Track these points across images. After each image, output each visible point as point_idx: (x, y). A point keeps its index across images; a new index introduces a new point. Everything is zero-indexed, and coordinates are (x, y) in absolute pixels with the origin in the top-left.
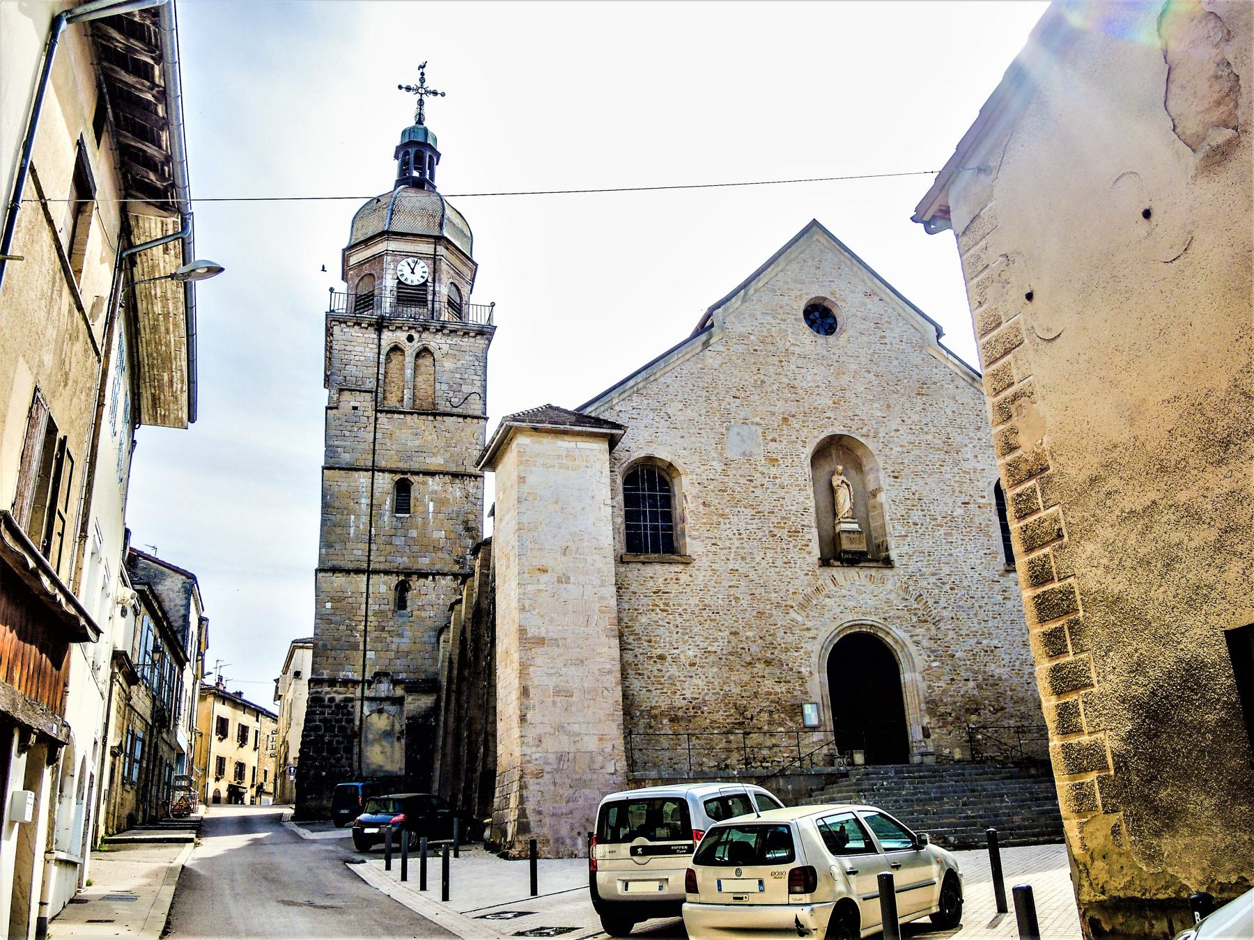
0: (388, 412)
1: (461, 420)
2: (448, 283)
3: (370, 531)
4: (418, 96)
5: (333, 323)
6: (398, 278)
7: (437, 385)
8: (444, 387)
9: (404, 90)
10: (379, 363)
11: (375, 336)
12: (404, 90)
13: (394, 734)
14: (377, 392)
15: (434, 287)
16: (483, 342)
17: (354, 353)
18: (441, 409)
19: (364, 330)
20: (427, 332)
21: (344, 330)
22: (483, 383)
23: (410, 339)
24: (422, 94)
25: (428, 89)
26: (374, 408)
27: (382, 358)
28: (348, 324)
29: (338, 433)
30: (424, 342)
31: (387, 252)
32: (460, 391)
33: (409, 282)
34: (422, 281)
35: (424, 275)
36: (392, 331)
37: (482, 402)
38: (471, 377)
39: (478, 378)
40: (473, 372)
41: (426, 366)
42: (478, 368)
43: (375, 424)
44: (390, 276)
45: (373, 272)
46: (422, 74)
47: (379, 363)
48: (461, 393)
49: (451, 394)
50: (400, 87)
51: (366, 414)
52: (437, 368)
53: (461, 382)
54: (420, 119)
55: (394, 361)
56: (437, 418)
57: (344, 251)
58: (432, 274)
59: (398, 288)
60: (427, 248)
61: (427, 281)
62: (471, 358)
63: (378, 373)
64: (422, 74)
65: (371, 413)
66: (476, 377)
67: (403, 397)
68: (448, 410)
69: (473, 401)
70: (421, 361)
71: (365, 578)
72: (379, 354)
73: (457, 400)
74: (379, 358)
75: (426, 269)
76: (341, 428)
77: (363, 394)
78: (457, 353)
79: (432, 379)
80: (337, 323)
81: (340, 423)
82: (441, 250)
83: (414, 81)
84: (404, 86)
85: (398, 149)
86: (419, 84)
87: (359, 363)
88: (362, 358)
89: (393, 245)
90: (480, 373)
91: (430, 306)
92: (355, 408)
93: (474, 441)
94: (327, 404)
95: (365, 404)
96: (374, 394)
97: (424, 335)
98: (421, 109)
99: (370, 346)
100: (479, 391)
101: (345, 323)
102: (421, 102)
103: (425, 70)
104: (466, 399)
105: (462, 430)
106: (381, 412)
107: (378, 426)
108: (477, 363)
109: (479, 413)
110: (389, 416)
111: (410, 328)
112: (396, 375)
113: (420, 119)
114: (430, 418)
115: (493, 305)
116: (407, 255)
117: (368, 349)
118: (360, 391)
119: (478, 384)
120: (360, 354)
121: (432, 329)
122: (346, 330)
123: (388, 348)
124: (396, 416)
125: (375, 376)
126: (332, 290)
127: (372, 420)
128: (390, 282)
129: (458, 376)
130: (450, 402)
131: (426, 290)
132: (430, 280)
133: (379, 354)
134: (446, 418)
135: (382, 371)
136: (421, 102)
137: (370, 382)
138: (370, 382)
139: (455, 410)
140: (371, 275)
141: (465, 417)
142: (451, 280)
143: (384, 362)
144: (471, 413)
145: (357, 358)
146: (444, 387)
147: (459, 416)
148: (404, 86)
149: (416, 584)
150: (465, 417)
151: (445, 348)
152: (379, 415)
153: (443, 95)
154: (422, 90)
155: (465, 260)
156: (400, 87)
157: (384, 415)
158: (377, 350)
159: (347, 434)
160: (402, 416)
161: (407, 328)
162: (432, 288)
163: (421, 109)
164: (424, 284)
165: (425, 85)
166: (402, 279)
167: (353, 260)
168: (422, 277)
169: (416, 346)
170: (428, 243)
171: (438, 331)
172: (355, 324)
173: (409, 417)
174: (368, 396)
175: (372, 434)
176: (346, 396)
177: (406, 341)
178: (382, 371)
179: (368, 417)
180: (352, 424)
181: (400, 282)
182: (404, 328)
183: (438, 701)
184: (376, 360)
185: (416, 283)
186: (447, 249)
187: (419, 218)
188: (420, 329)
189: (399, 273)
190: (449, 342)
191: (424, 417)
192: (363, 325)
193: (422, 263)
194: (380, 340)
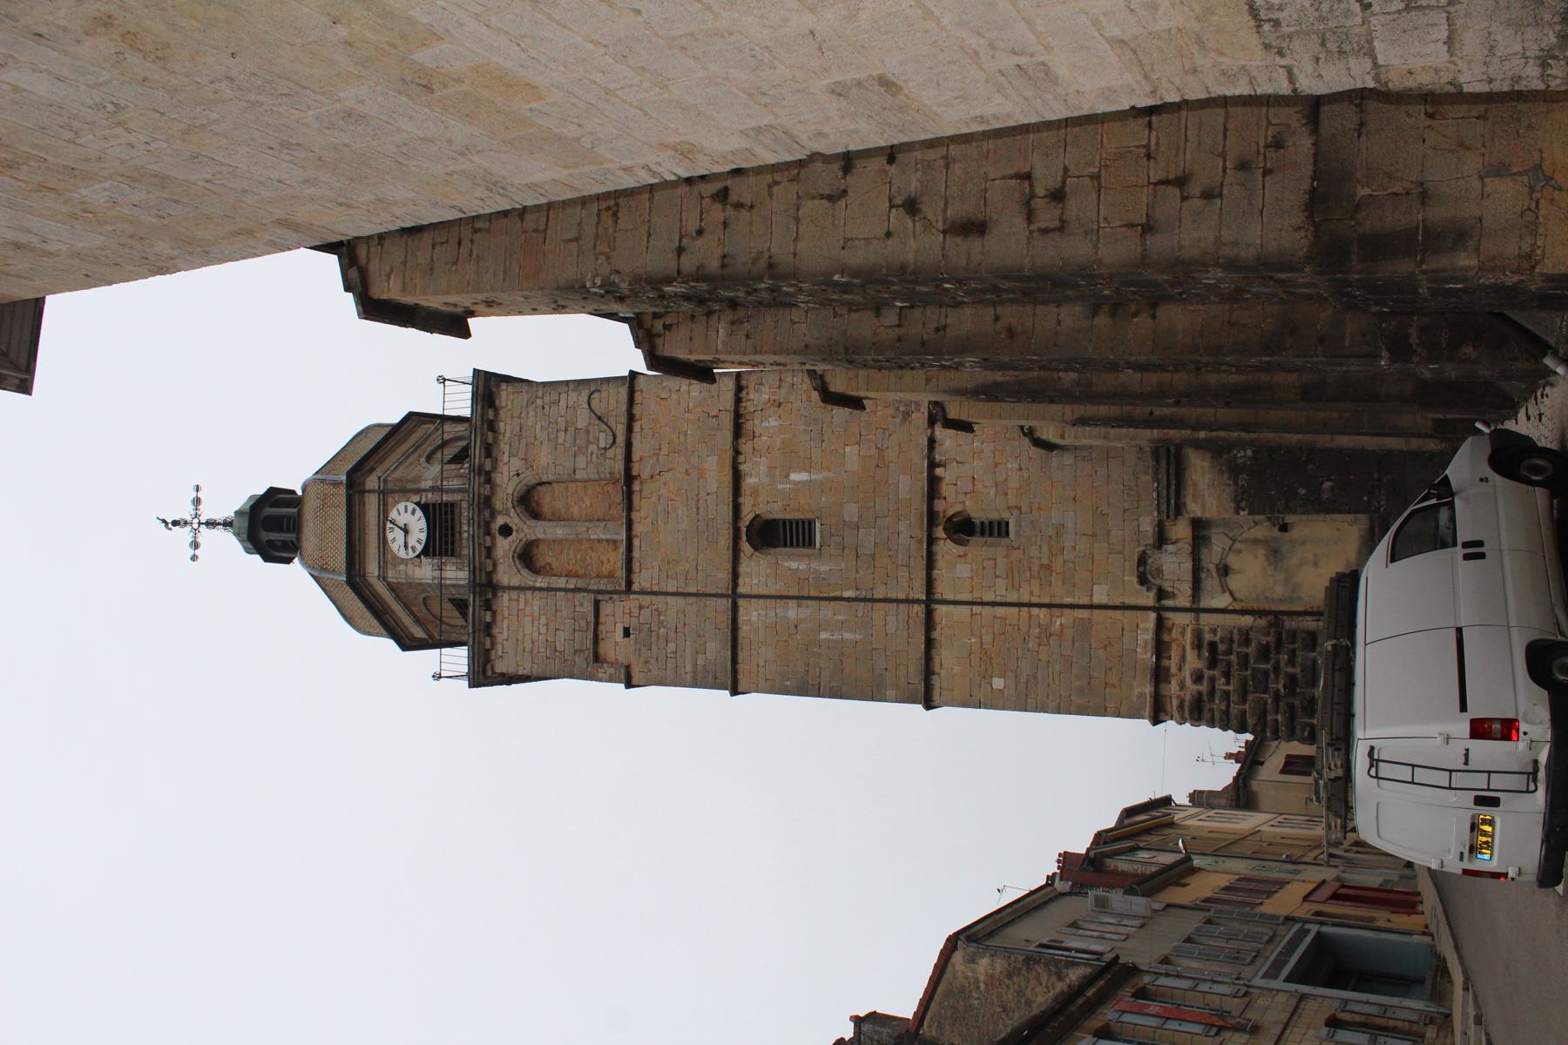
0: (629, 570)
1: (637, 427)
2: (425, 465)
3: (849, 600)
4: (203, 528)
5: (489, 673)
6: (418, 556)
7: (579, 476)
8: (581, 462)
9: (197, 552)
10: (548, 589)
11: (506, 596)
12: (197, 552)
13: (1275, 539)
14: (598, 592)
15: (426, 491)
16: (504, 394)
17: (536, 634)
18: (619, 466)
19: (499, 617)
20: (494, 500)
21: (500, 652)
22: (571, 387)
23: (506, 531)
24: (200, 523)
25: (193, 513)
26: (624, 597)
27: (540, 582)
28: (488, 645)
29: (671, 664)
30: (510, 505)
31: (383, 577)
32: (588, 432)
33: (423, 536)
34: (419, 513)
35: (410, 510)
36: (495, 565)
37: (605, 386)
38: (563, 411)
39: (564, 396)
40: (554, 408)
41: (553, 498)
42: (547, 399)
43: (652, 593)
44: (417, 569)
45: (420, 600)
46: (175, 523)
47: (548, 589)
48: (591, 429)
49: (593, 448)
50: (194, 558)
51: (635, 612)
52: (551, 478)
53: (571, 429)
54: (227, 524)
55: (548, 560)
56: (635, 473)
57: (405, 646)
58: (407, 495)
59: (434, 555)
60: (372, 503)
61: (418, 504)
62: (532, 414)
63: (565, 590)
64: (175, 523)
65: (633, 602)
66: (563, 403)
67: (608, 541)
68: (619, 451)
69: (604, 405)
70: (546, 509)
71: (941, 610)
72: (534, 589)
73: (602, 436)
74: (540, 589)
75: (401, 506)
76: (662, 659)
77: (602, 619)
78: (523, 442)
79: (572, 486)
80: (489, 666)
81: (653, 660)
82: (372, 482)
83: (184, 534)
84: (192, 552)
85: (268, 558)
86: (188, 528)
87: (552, 625)
88: (543, 620)
89: (372, 569)
90: (555, 396)
91: (456, 497)
92: (627, 632)
93: (674, 397)
94: (623, 685)
95: (619, 614)
96: (600, 597)
97: (498, 505)
98: (219, 524)
99: (521, 607)
100: (585, 393)
101: (488, 651)
102: (211, 524)
103: (169, 521)
104: (600, 418)
105: (655, 421)
106: (629, 583)
107: (655, 589)
108: (539, 402)
109: (624, 391)
110: (636, 567)
111: (488, 532)
112: (571, 554)
113: (227, 524)
114: (636, 486)
115: (443, 380)
116: (383, 541)
117: (528, 610)
118: (597, 623)
119: (573, 396)
120: (536, 623)
121: (486, 490)
122: (499, 648)
123: (524, 572)
124: (636, 554)
125: (570, 595)
126: (438, 677)
127: (646, 600)
128: (426, 572)
129: (562, 435)
130: (605, 449)
131: (434, 505)
132: (417, 499)
133: (534, 589)
134: (635, 457)
135: (561, 582)
136: (211, 524)
137: (582, 605)
138: (582, 605)
139: (621, 439)
140: (424, 599)
141: (631, 418)
142: (423, 460)
143: (547, 579)
144: (623, 407)
145: (543, 630)
146: (581, 462)
147: (630, 429)
148: (192, 552)
149: (952, 502)
150: (631, 418)
151: (516, 464)
152: (636, 587)
153: (198, 489)
154: (192, 523)
155: (398, 436)
156: (194, 558)
157: (635, 578)
158: (529, 594)
159: (671, 647)
160: (636, 542)
161: (488, 538)
162: (430, 495)
163: (219, 524)
164: (425, 508)
165: (189, 519)
166: (420, 548)
167: (419, 633)
168: (413, 512)
169: (517, 520)
170: (362, 504)
171: (489, 480)
172: (489, 635)
173: (638, 528)
174: (606, 609)
175: (670, 599)
176: (606, 649)
177: (510, 538)
178: (561, 582)
179: (641, 607)
180: (654, 638)
181: (425, 552)
182: (488, 544)
183: (1197, 445)
184: (544, 594)
185: (423, 524)
186: (372, 470)
187: (330, 522)
188: (487, 514)
189: (412, 555)
190: (505, 458)
191: (636, 498)
192: (488, 619)
193: (393, 515)
194: (510, 588)
